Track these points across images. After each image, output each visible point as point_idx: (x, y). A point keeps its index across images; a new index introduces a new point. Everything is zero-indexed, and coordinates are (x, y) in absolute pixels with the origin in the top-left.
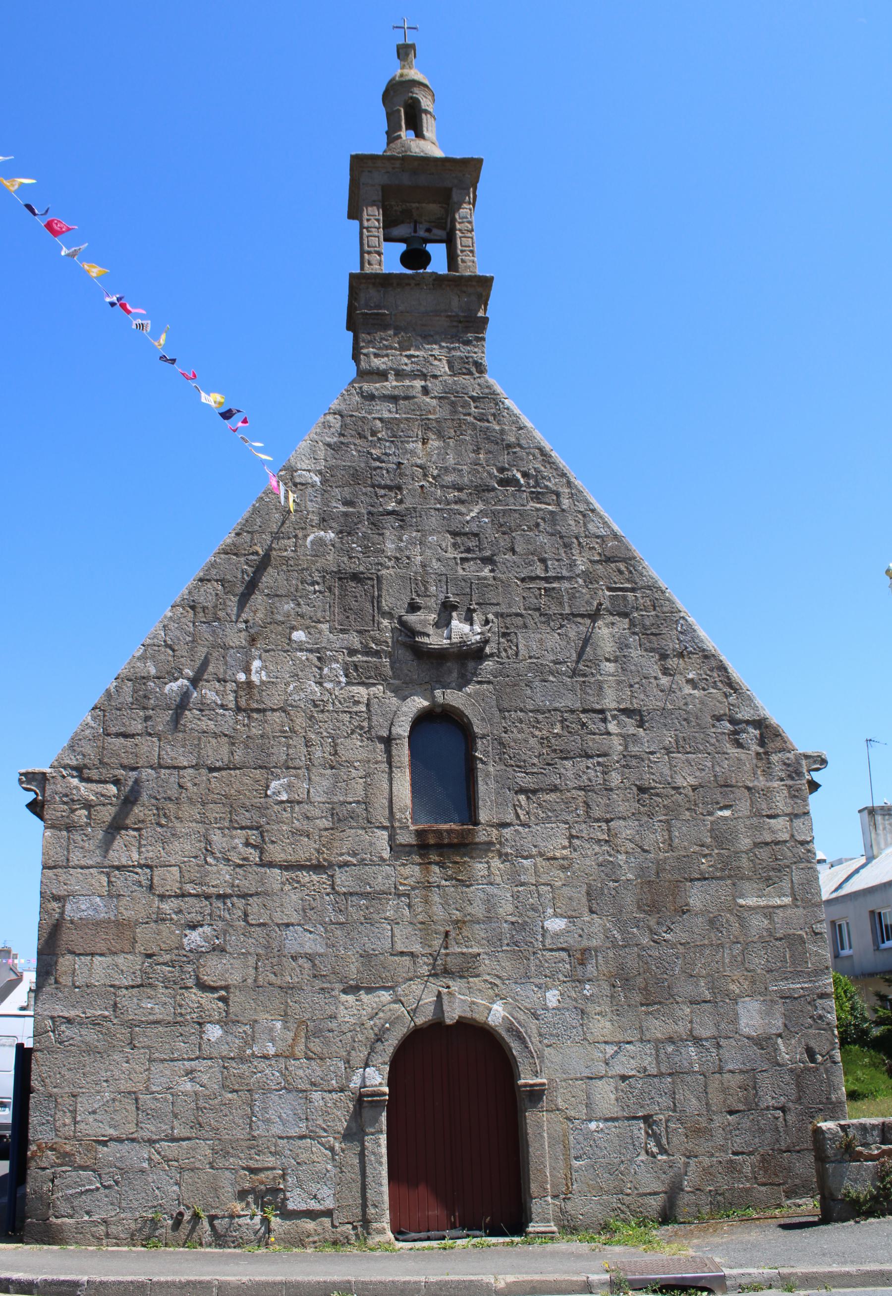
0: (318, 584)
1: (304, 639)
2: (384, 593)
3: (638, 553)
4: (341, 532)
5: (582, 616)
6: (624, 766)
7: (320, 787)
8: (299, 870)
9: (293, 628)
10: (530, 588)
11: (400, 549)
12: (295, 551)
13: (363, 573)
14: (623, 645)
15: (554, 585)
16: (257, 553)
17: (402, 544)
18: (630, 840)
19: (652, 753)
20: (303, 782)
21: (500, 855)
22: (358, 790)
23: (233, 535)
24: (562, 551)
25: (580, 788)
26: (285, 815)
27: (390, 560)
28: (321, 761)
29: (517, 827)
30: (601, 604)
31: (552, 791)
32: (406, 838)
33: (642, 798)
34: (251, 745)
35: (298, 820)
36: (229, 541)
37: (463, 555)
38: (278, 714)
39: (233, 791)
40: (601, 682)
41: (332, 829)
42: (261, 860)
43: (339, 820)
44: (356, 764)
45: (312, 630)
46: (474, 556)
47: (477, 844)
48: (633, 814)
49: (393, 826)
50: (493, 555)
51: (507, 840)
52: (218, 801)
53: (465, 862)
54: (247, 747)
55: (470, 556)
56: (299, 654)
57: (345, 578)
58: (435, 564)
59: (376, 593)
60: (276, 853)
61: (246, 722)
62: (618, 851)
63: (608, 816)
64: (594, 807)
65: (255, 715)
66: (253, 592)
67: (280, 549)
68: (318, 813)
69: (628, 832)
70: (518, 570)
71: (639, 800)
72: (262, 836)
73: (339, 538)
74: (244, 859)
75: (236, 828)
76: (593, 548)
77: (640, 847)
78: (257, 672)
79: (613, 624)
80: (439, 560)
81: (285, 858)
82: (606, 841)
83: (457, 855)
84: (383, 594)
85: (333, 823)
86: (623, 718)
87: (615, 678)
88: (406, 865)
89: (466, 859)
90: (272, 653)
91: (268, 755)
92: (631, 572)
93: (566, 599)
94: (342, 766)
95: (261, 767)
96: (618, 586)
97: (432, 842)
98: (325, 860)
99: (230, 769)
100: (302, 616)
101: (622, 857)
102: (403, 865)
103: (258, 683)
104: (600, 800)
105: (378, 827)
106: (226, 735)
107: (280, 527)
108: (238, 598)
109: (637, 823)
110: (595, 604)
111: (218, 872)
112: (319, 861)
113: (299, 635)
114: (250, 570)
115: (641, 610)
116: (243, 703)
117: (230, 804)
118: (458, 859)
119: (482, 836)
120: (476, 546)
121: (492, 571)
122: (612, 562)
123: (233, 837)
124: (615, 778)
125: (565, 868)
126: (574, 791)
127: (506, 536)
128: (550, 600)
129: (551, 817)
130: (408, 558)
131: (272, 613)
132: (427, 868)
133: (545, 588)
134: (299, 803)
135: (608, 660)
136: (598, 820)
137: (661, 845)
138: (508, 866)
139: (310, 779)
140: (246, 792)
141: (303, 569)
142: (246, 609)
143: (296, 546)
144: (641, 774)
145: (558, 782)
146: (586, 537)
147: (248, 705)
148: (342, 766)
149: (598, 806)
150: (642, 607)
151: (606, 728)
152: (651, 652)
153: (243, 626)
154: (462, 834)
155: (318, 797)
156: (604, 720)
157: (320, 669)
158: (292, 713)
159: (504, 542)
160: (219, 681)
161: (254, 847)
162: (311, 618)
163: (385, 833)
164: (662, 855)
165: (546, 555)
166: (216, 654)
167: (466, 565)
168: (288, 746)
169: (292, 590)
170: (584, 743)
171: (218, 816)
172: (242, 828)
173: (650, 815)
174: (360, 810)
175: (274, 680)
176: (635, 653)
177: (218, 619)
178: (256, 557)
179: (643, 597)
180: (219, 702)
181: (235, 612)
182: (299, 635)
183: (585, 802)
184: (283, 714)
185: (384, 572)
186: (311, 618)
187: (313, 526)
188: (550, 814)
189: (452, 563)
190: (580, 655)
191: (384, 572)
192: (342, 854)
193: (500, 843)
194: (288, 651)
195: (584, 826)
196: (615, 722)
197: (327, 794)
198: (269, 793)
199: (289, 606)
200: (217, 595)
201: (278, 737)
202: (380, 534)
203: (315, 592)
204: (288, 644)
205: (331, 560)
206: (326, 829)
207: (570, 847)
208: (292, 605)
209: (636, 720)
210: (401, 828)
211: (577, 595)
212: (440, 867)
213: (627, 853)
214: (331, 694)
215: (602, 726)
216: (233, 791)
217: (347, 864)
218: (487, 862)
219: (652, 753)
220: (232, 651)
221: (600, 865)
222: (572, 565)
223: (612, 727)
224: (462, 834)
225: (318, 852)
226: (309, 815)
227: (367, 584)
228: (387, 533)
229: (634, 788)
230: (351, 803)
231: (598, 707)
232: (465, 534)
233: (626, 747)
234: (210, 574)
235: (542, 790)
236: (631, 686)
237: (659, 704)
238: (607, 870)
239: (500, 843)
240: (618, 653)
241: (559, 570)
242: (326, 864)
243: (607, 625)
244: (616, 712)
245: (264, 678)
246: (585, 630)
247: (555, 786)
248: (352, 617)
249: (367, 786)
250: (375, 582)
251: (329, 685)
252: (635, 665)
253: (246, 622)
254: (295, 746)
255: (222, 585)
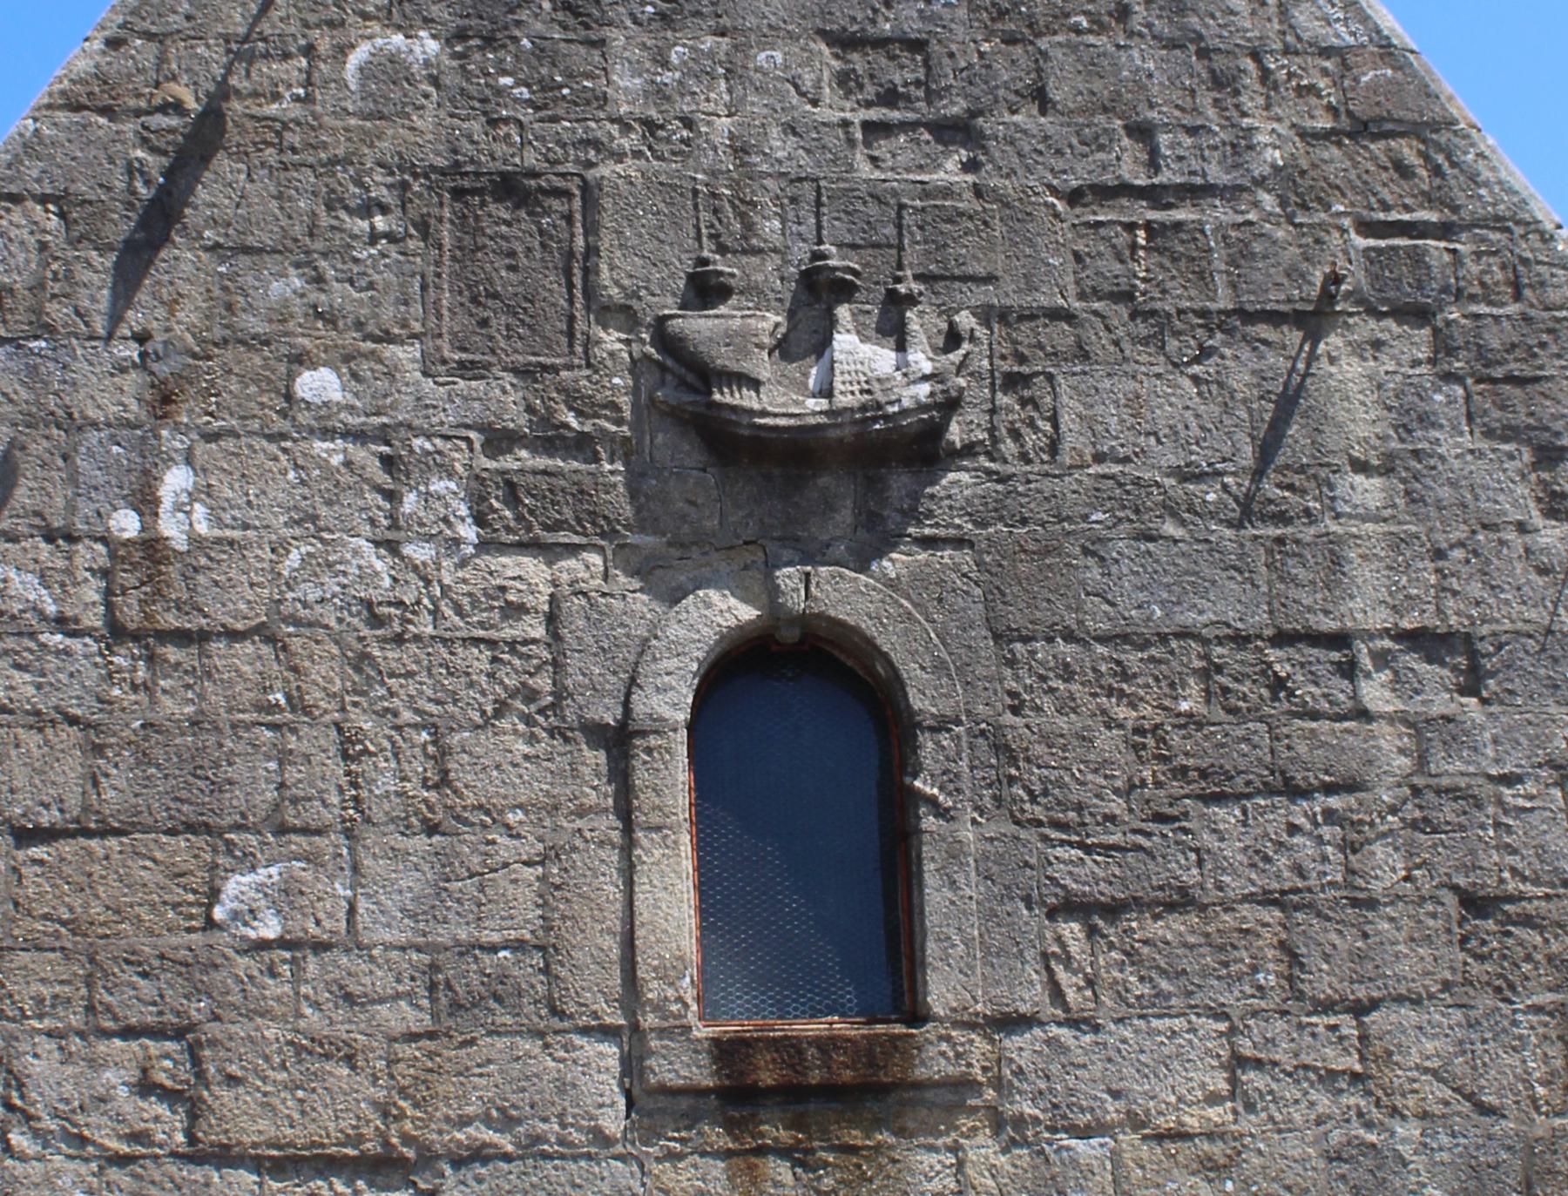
0: (384, 209)
1: (337, 396)
2: (606, 241)
3: (1463, 105)
4: (461, 35)
5: (1274, 318)
6: (1414, 825)
7: (390, 895)
8: (321, 1174)
9: (301, 360)
10: (1099, 224)
11: (659, 94)
12: (308, 100)
13: (535, 174)
14: (1411, 417)
15: (1180, 215)
16: (177, 107)
17: (668, 77)
18: (1434, 1073)
19: (1509, 780)
20: (332, 877)
21: (998, 1122)
22: (518, 904)
23: (98, 45)
24: (1205, 100)
25: (1267, 899)
26: (274, 988)
27: (626, 128)
28: (396, 807)
29: (1054, 1030)
30: (1336, 279)
31: (1171, 907)
32: (678, 1066)
33: (1474, 933)
34: (159, 754)
35: (317, 1005)
36: (83, 65)
37: (874, 114)
38: (249, 648)
39: (96, 909)
40: (1337, 540)
41: (431, 1035)
42: (192, 1139)
43: (456, 1006)
44: (511, 818)
45: (364, 367)
46: (911, 116)
47: (918, 1085)
48: (1446, 986)
49: (635, 1028)
50: (973, 114)
51: (1019, 1073)
52: (48, 941)
53: (878, 1148)
54: (144, 759)
55: (895, 115)
56: (320, 446)
57: (473, 192)
58: (779, 145)
59: (580, 242)
60: (243, 1116)
61: (142, 674)
62: (1395, 1112)
63: (1361, 992)
64: (1314, 960)
65: (172, 653)
66: (166, 239)
67: (255, 94)
68: (382, 981)
69: (1429, 1046)
70: (1059, 164)
71: (1464, 940)
72: (196, 1061)
73: (455, 56)
74: (136, 1137)
75: (107, 1034)
76: (1312, 90)
77: (1469, 1097)
78: (178, 507)
79: (1377, 345)
80: (791, 129)
81: (273, 1132)
82: (1356, 1077)
83: (852, 1124)
84: (604, 245)
85: (435, 1016)
86: (1412, 661)
87: (1383, 528)
88: (680, 1157)
89: (884, 1137)
90: (229, 444)
91: (217, 788)
92: (1437, 171)
93: (1218, 260)
94: (466, 822)
95: (191, 828)
96: (1394, 216)
97: (767, 1078)
98: (407, 1139)
99: (88, 833)
100: (330, 319)
101: (1408, 1131)
102: (672, 1156)
103: (180, 543)
104: (1333, 936)
105: (585, 1031)
106: (73, 721)
107: (257, 19)
108: (113, 257)
109: (1457, 1015)
110: (1318, 277)
111: (48, 1181)
112: (386, 1144)
113: (319, 384)
114: (155, 164)
115: (1473, 298)
116: (131, 613)
117: (89, 952)
118: (855, 1137)
119: (936, 1059)
120: (918, 83)
121: (971, 166)
122: (1375, 137)
123: (95, 1064)
124: (1385, 866)
125: (1216, 1168)
126: (1245, 910)
127: (1018, 51)
128: (1167, 267)
129: (1168, 996)
130: (688, 123)
131: (229, 307)
132: (752, 1167)
133: (1148, 227)
134: (320, 947)
135: (1361, 467)
136: (1326, 1007)
137: (1541, 1090)
138: (1025, 1162)
139: (356, 868)
140: (143, 912)
141: (333, 161)
142: (142, 296)
143: (308, 83)
144: (1472, 852)
145: (1192, 876)
146: (1287, 51)
147: (148, 617)
148: (466, 822)
149: (1327, 958)
150: (1476, 289)
151: (1355, 697)
152: (1506, 439)
153: (131, 351)
154: (870, 1053)
155: (384, 927)
156: (1349, 670)
157: (392, 496)
158: (296, 644)
159: (1009, 70)
160: (50, 539)
161: (170, 1096)
162: (359, 325)
163: (610, 1050)
164: (1542, 1125)
165: (1153, 114)
166: (38, 447)
167: (882, 148)
168: (284, 757)
169: (298, 230)
170: (1280, 747)
171: (46, 991)
172: (128, 1033)
173: (1504, 990)
174: (525, 971)
175: (237, 534)
176: (1452, 443)
177: (48, 330)
178: (173, 121)
179: (1478, 255)
180: (51, 609)
181: (104, 305)
182: (319, 384)
183: (1282, 945)
184: (266, 650)
185: (605, 170)
186: (359, 325)
187: (366, 16)
188: (1164, 985)
189: (834, 140)
190: (1267, 449)
191: (605, 170)
192: (464, 1121)
193: (998, 1083)
194: (283, 436)
195: (1280, 1024)
196: (1385, 676)
197: (413, 916)
198: (219, 913)
199: (286, 286)
200: (43, 246)
201: (248, 726)
202: (592, 44)
203: (374, 237)
204: (283, 414)
205: (426, 130)
206: (412, 1037)
207: (1232, 1096)
208: (298, 283)
209: (1454, 668)
210: (662, 1032)
211: (1257, 247)
212: (796, 1163)
213: (1424, 1116)
214: (428, 583)
215: (1339, 688)
216: (96, 909)
217: (480, 1154)
218: (955, 1149)
219: (1509, 780)
220: (93, 437)
221: (1333, 1157)
222: (1241, 146)
223: (1376, 692)
224: (869, 1053)
225: (385, 1115)
226: (352, 988)
227: (548, 212)
228: (617, 38)
229: (1450, 899)
230: (493, 949)
231: (1328, 625)
232: (881, 43)
233: (1422, 761)
234: (19, 176)
235: (1136, 904)
236: (1439, 554)
237: (1532, 614)
238: (1359, 1175)
239: (998, 1083)
240: (1394, 445)
241: (1195, 165)
242: (410, 1153)
243: (1357, 350)
244: (1387, 643)
245: (203, 528)
246: (1283, 364)
247: (1183, 890)
248: (499, 322)
249: (549, 890)
250: (577, 203)
251: (420, 552)
252: (1453, 484)
253: (142, 338)
254: (307, 758)
255: (62, 215)
